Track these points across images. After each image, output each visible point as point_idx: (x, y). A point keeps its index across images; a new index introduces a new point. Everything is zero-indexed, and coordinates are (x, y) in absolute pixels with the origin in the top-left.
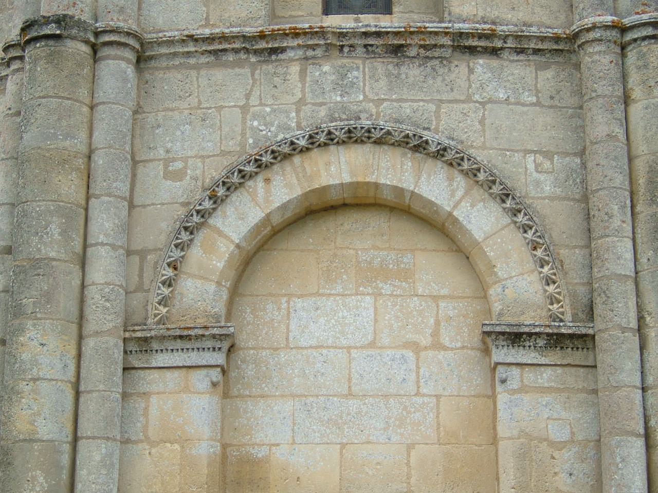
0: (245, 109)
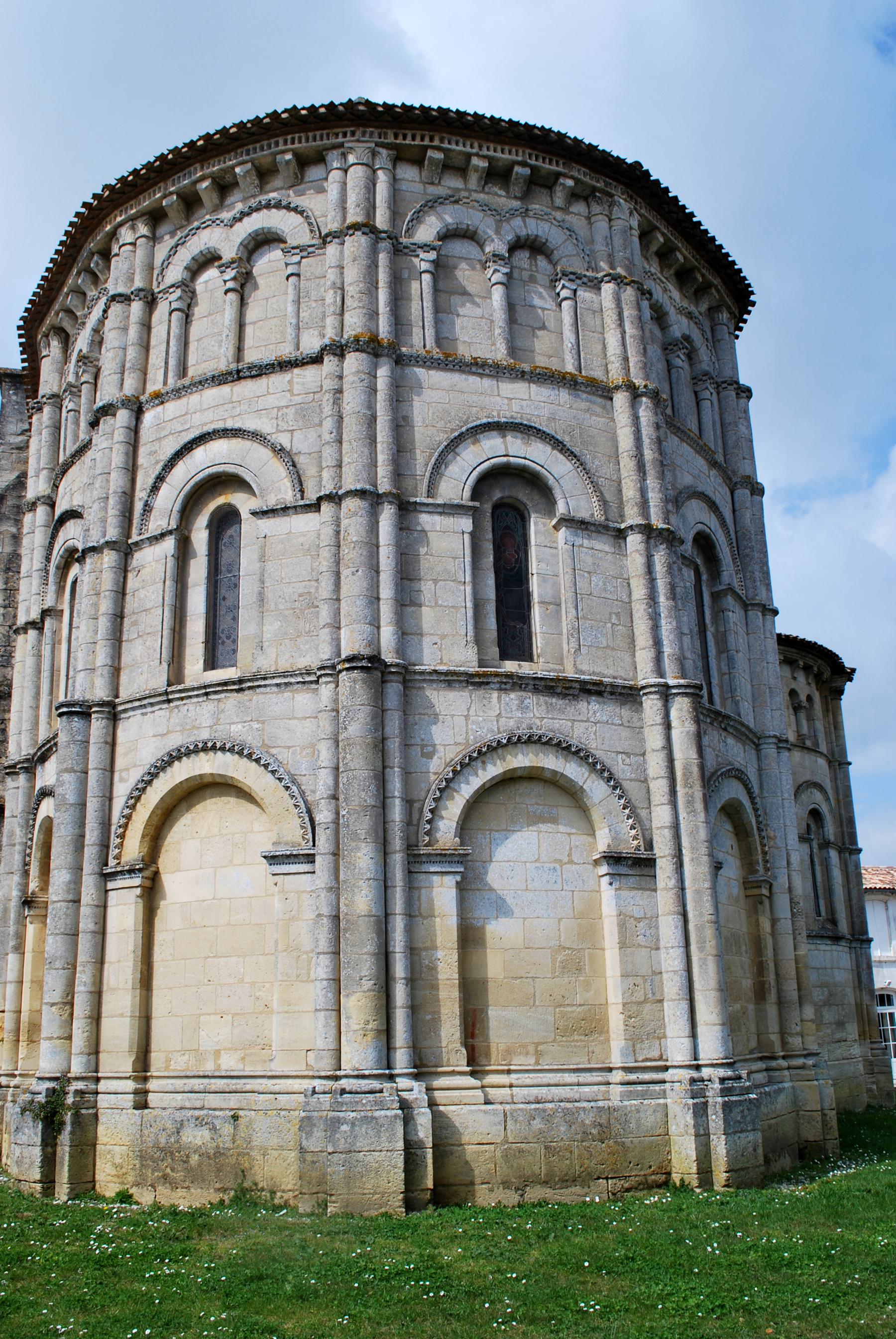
0: (467, 717)
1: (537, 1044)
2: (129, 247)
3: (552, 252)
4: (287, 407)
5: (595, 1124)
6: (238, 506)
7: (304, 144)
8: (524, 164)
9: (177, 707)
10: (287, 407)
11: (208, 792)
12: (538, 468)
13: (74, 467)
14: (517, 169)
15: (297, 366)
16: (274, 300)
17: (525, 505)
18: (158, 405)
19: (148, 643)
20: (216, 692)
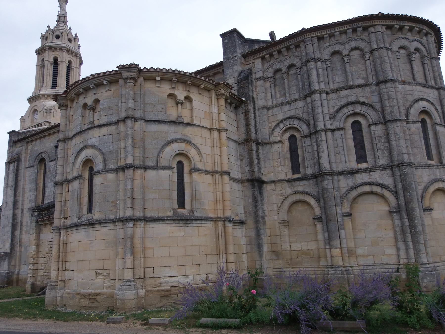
2: (381, 33)
19: (418, 150)
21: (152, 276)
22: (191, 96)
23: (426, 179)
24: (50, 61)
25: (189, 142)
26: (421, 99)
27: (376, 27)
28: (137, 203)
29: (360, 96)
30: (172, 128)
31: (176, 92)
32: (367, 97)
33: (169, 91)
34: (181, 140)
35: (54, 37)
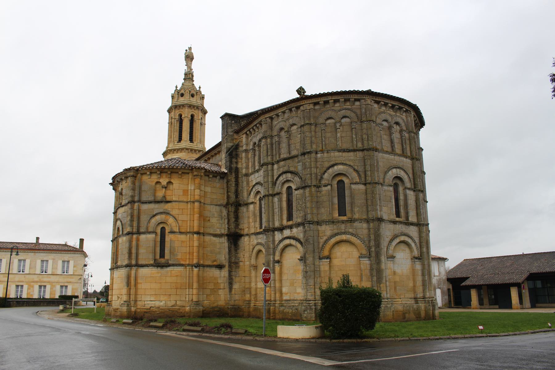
1: (404, 293)
2: (308, 110)
3: (400, 125)
4: (356, 160)
5: (416, 308)
6: (344, 180)
7: (356, 97)
8: (398, 105)
9: (335, 224)
10: (356, 160)
11: (343, 243)
12: (402, 177)
13: (289, 160)
14: (396, 106)
15: (358, 151)
16: (348, 132)
17: (398, 184)
18: (321, 153)
19: (326, 209)
20: (345, 222)
21: (140, 300)
22: (172, 181)
23: (329, 233)
24: (176, 119)
25: (167, 213)
26: (336, 164)
27: (304, 106)
28: (134, 256)
29: (291, 166)
30: (157, 206)
31: (161, 180)
32: (295, 167)
33: (156, 180)
34: (161, 213)
35: (180, 96)
